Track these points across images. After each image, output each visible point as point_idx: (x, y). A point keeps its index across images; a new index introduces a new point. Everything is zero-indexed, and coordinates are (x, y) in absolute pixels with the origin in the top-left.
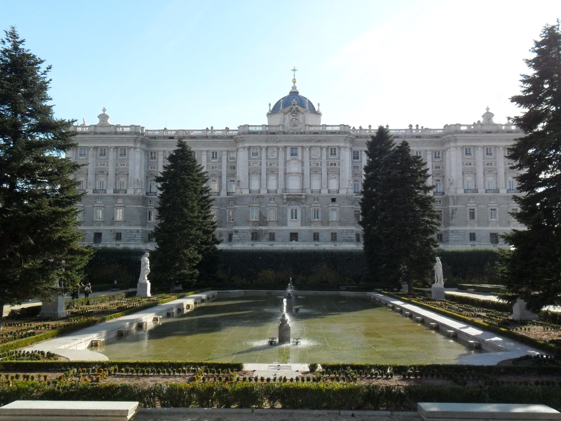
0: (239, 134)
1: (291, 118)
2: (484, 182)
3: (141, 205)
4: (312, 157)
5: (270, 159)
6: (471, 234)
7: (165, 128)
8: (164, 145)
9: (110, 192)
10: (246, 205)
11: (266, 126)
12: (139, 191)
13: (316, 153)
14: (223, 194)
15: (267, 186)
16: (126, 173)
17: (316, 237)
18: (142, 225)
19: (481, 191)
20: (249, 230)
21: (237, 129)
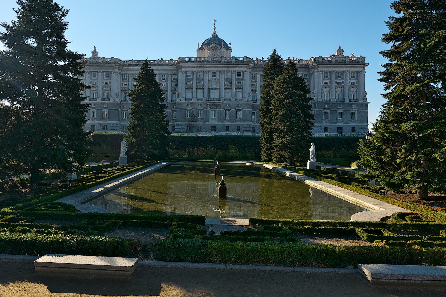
0: (179, 63)
1: (213, 52)
2: (335, 95)
3: (118, 108)
4: (225, 78)
5: (199, 79)
6: (325, 128)
7: (133, 59)
8: (132, 71)
9: (100, 100)
10: (183, 108)
11: (197, 58)
12: (117, 99)
13: (228, 76)
14: (169, 101)
15: (196, 97)
16: (110, 88)
17: (227, 128)
18: (119, 121)
19: (333, 100)
20: (185, 124)
21: (178, 60)
